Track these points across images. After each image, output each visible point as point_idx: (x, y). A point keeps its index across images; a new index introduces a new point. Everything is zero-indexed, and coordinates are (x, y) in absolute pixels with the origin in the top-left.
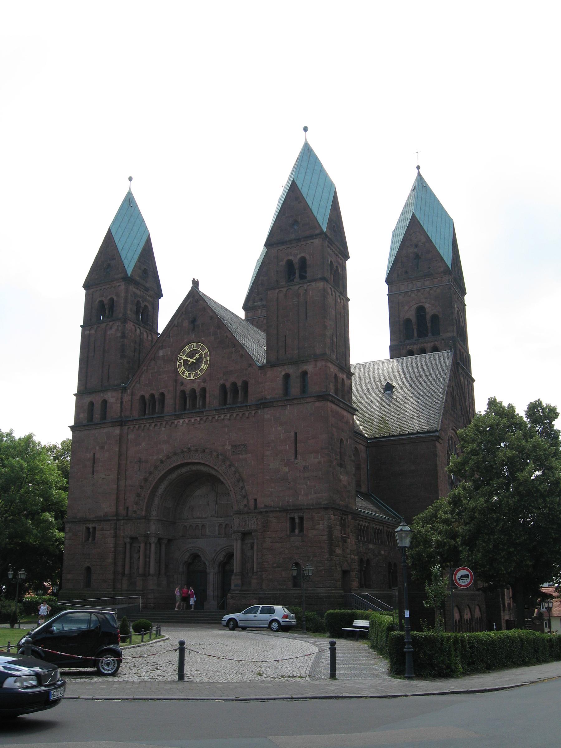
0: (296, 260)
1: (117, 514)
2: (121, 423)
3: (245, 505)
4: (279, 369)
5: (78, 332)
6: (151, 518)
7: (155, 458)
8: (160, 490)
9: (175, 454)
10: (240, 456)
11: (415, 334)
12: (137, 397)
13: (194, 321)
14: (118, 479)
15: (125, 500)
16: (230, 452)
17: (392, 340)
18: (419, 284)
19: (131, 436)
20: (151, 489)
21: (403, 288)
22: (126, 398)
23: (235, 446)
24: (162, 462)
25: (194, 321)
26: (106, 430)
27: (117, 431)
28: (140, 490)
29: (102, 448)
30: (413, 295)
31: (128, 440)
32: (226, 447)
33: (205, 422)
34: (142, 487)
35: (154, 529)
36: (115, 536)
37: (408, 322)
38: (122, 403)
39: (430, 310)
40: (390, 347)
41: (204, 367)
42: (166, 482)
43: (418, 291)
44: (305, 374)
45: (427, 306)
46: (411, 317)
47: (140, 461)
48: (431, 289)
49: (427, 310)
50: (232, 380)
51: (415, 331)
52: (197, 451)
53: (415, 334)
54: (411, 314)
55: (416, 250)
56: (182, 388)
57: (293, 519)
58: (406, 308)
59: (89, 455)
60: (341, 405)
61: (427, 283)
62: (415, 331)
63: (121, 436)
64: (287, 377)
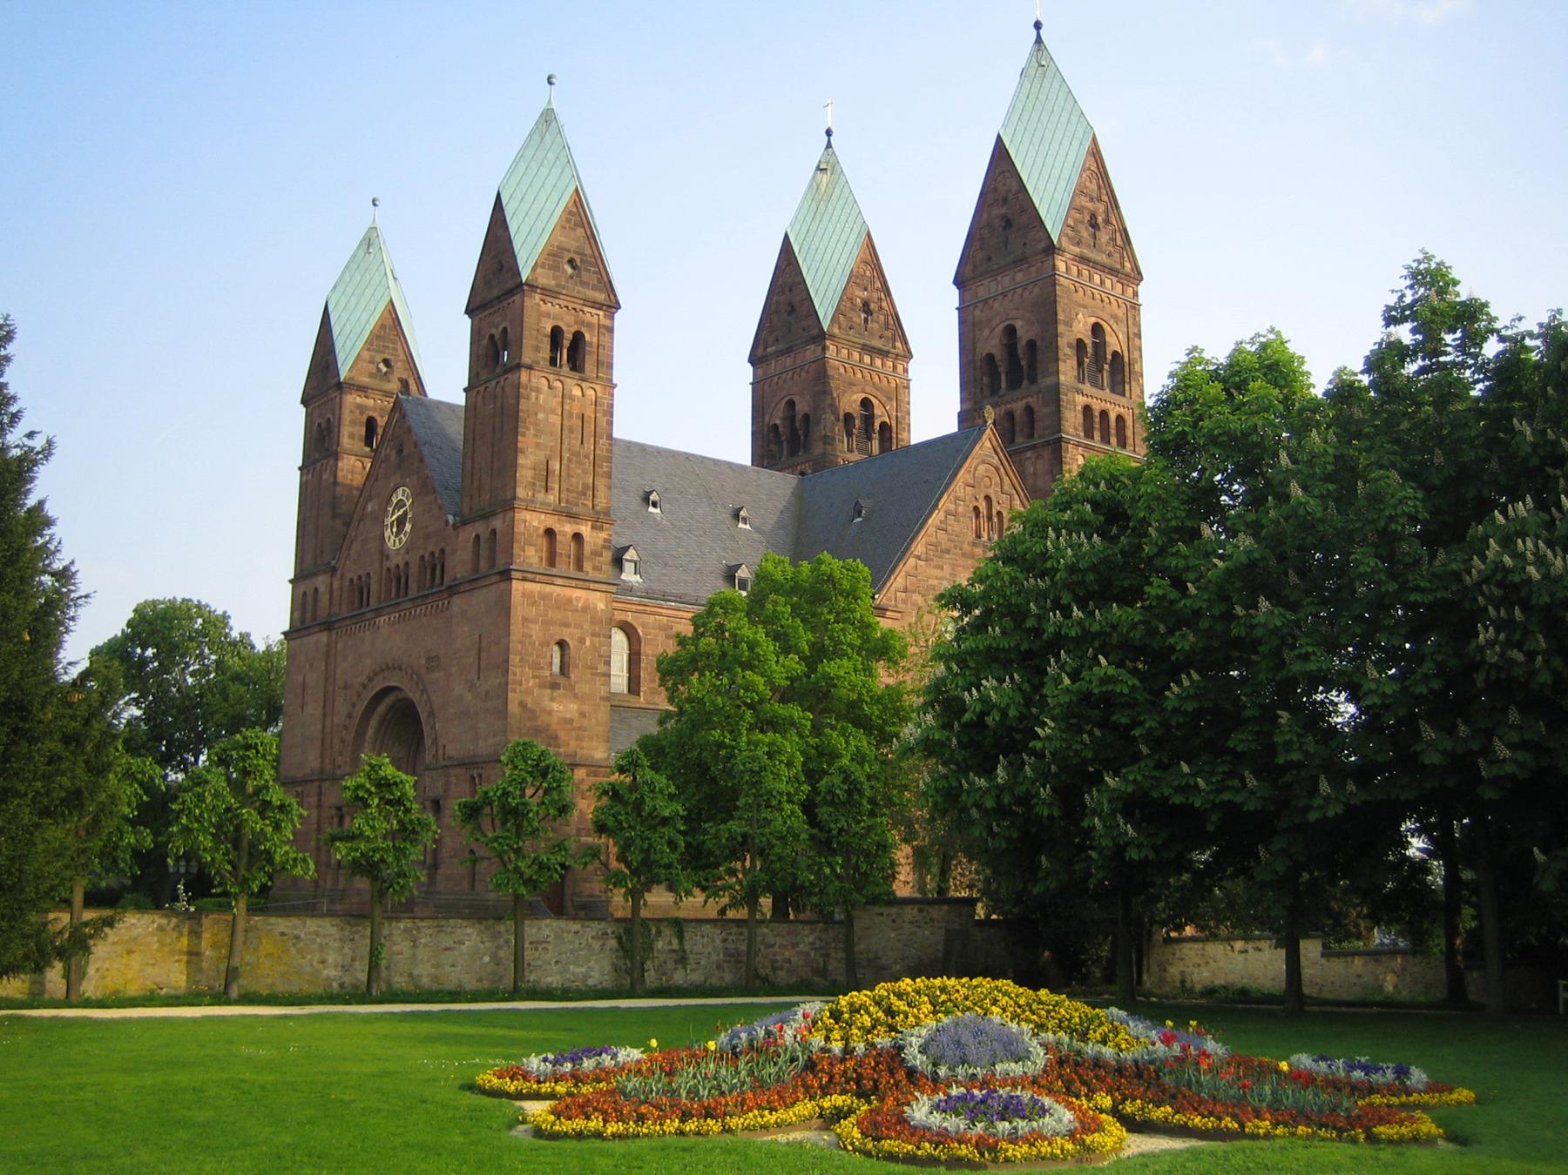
0: (497, 333)
1: (322, 771)
2: (328, 626)
4: (469, 528)
5: (295, 478)
8: (370, 733)
11: (1003, 385)
12: (347, 583)
13: (400, 451)
14: (324, 715)
17: (962, 401)
18: (1007, 280)
19: (340, 646)
21: (982, 293)
22: (336, 584)
23: (428, 659)
24: (364, 686)
25: (400, 451)
26: (315, 637)
27: (323, 638)
29: (311, 665)
30: (996, 305)
36: (319, 806)
37: (990, 357)
38: (331, 592)
39: (1024, 333)
40: (960, 414)
41: (408, 527)
43: (1004, 295)
44: (494, 532)
45: (1018, 324)
46: (994, 351)
48: (1025, 288)
49: (1019, 333)
50: (431, 548)
51: (1003, 376)
53: (1003, 385)
54: (992, 343)
55: (1003, 210)
56: (387, 564)
57: (473, 778)
58: (986, 332)
59: (300, 679)
60: (559, 581)
61: (1019, 276)
62: (1003, 376)
63: (328, 645)
64: (477, 536)
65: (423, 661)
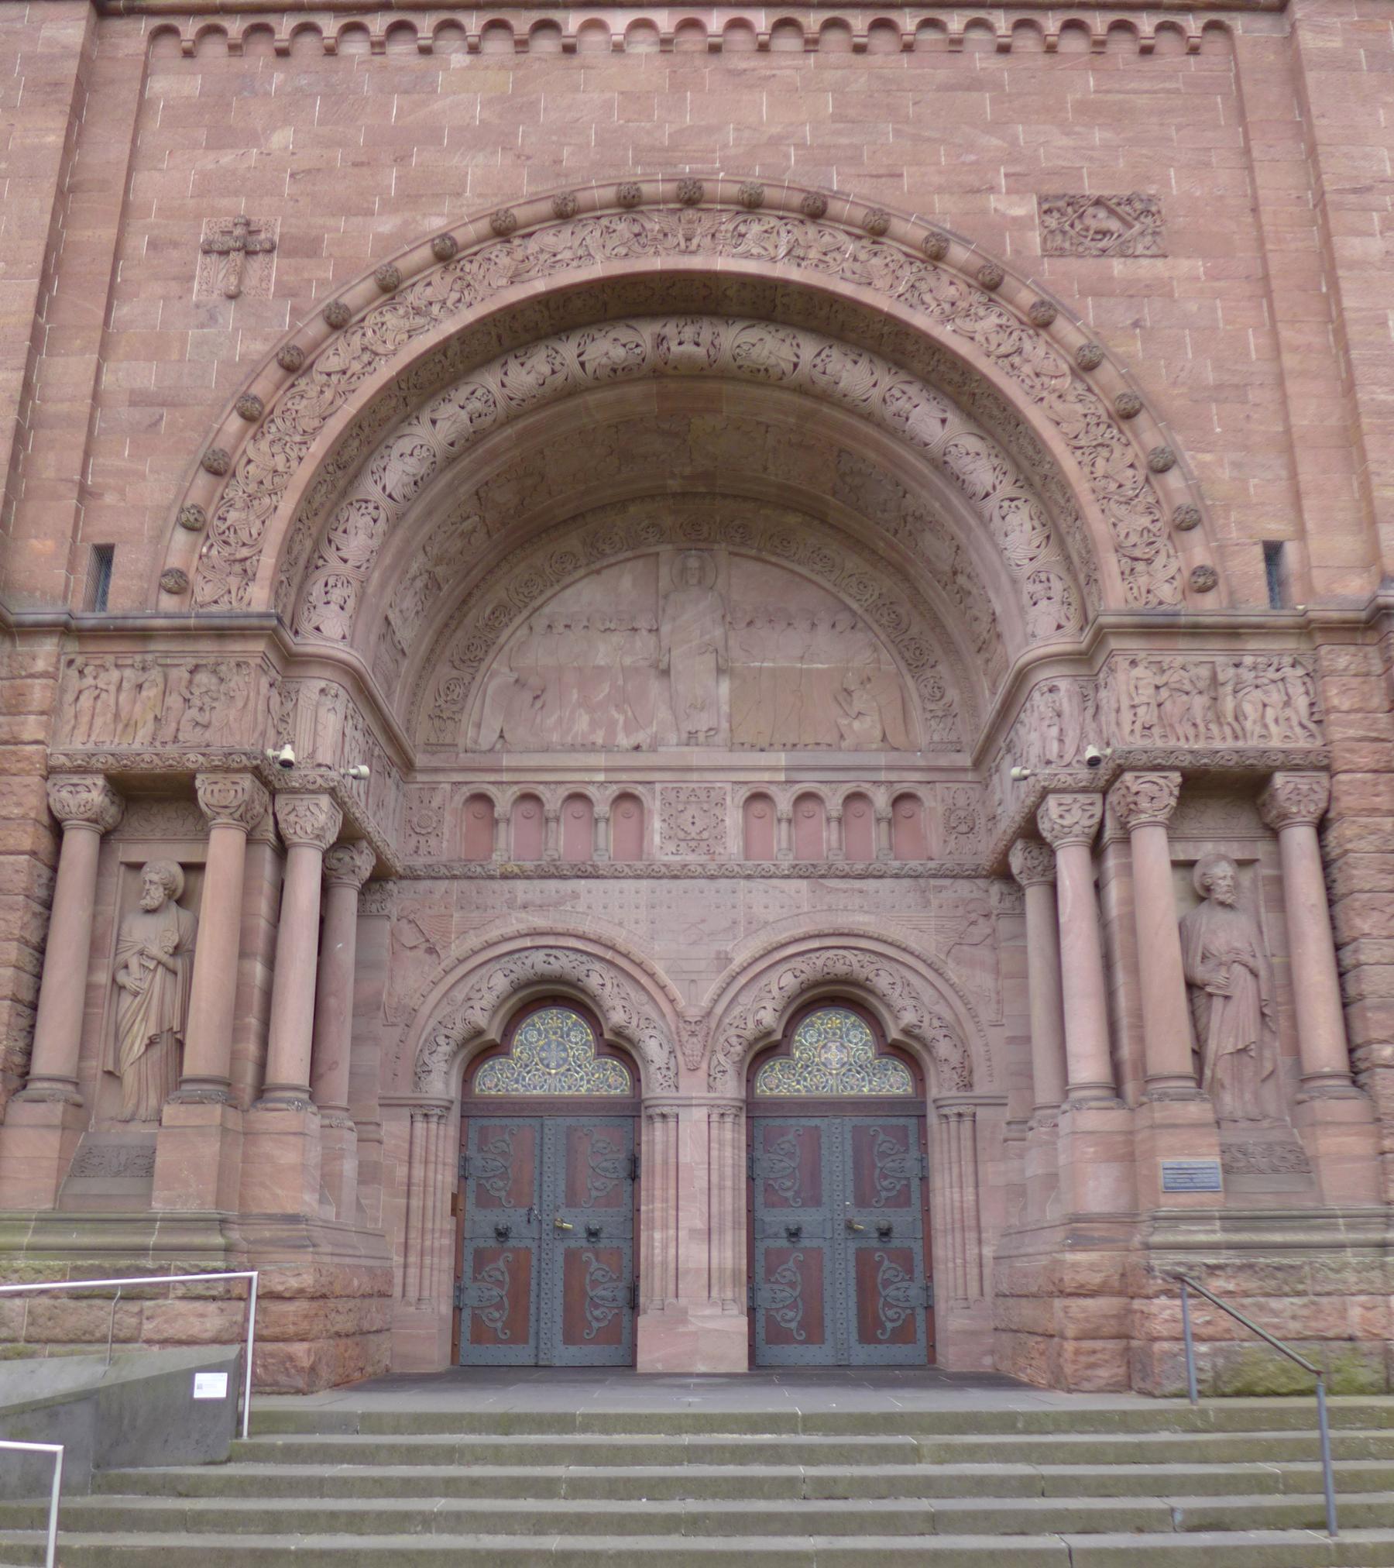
3: (1204, 581)
6: (310, 644)
7: (386, 225)
9: (565, 214)
10: (1118, 267)
15: (84, 493)
16: (1035, 238)
20: (336, 426)
28: (235, 423)
31: (143, 106)
32: (993, 202)
33: (812, 45)
34: (253, 416)
35: (321, 734)
42: (445, 422)
47: (245, 244)
52: (752, 205)
65: (1024, 208)
